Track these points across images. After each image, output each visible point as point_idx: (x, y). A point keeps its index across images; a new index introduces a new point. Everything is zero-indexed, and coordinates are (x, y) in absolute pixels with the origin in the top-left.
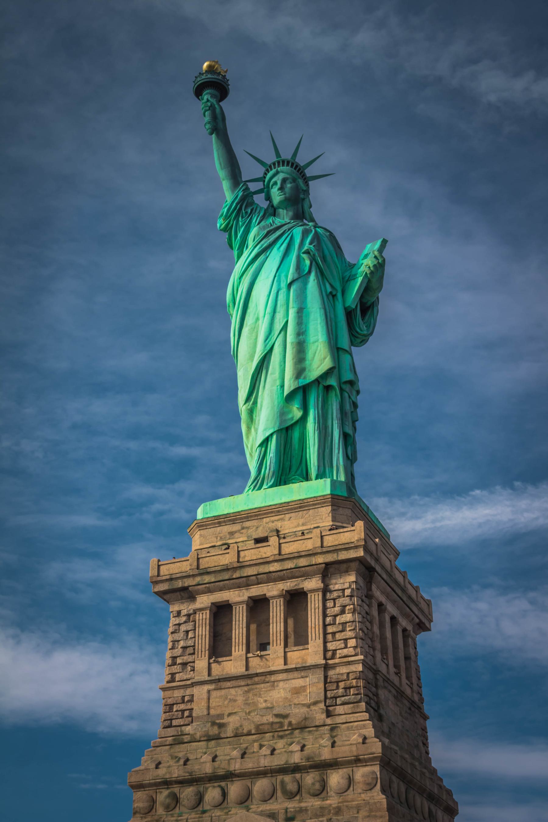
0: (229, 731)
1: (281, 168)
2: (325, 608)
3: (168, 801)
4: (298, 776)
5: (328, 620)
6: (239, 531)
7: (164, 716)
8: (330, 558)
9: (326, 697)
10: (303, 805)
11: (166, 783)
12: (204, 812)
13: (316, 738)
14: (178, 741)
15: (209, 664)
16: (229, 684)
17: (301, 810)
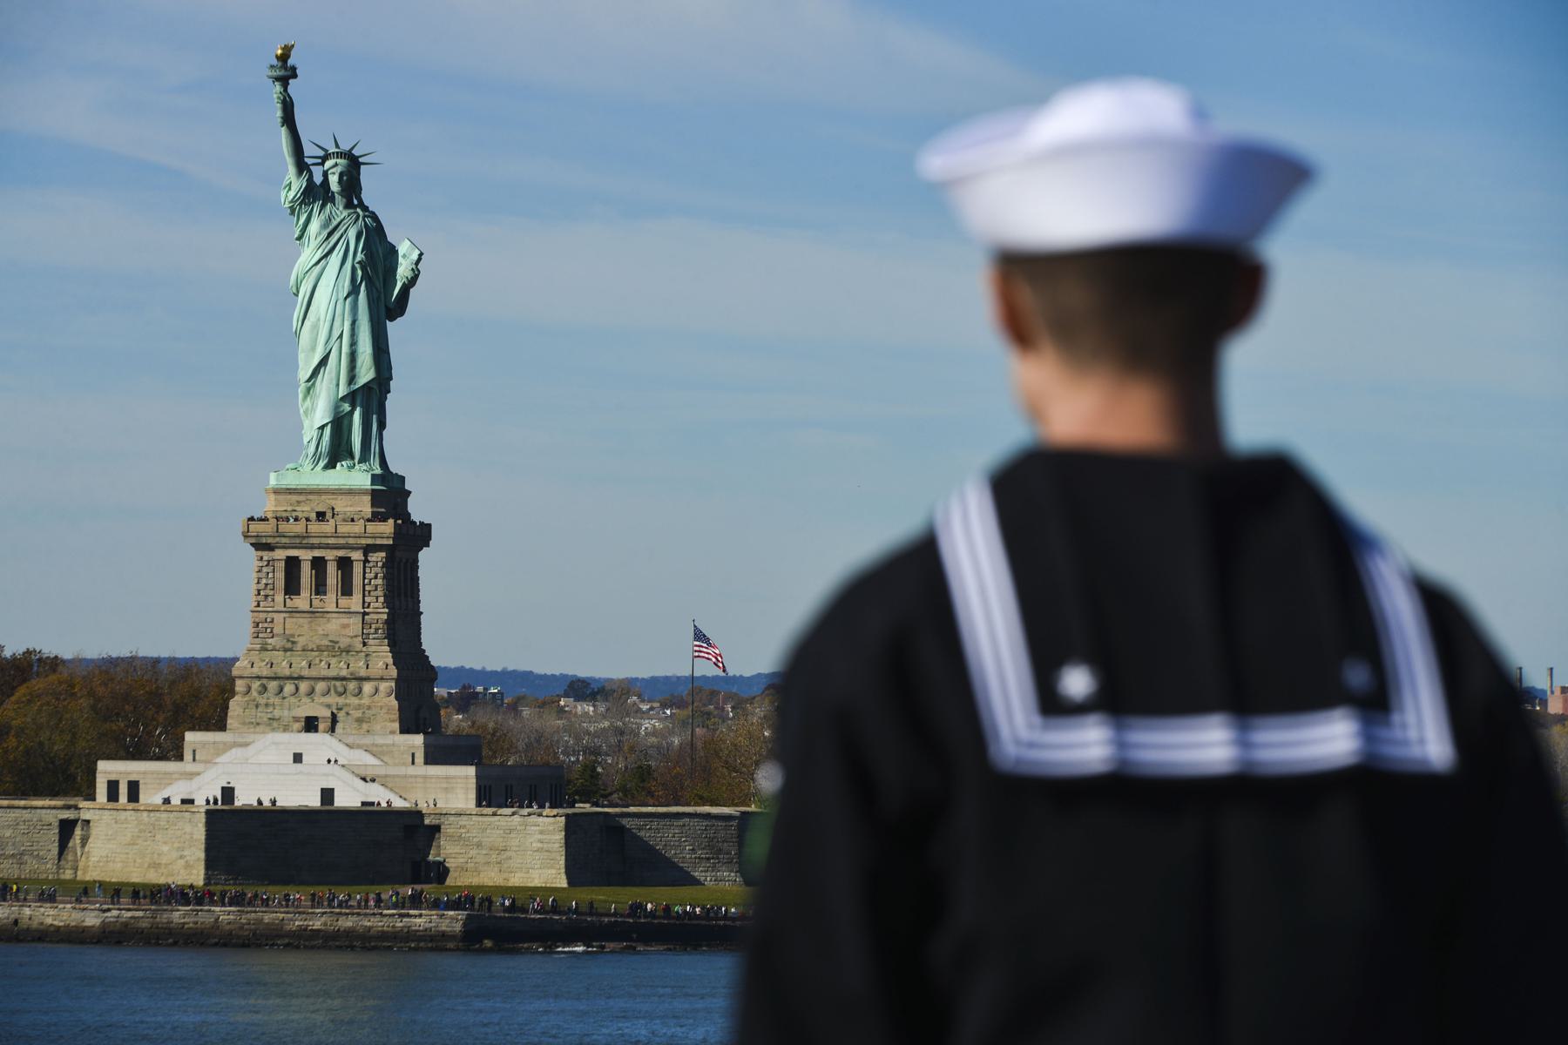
0: (299, 647)
1: (339, 161)
2: (364, 573)
3: (260, 689)
4: (344, 683)
5: (366, 581)
6: (304, 501)
7: (253, 630)
8: (370, 541)
9: (363, 633)
10: (348, 701)
11: (259, 678)
12: (284, 698)
13: (356, 661)
14: (264, 649)
15: (285, 599)
16: (298, 615)
17: (346, 705)
